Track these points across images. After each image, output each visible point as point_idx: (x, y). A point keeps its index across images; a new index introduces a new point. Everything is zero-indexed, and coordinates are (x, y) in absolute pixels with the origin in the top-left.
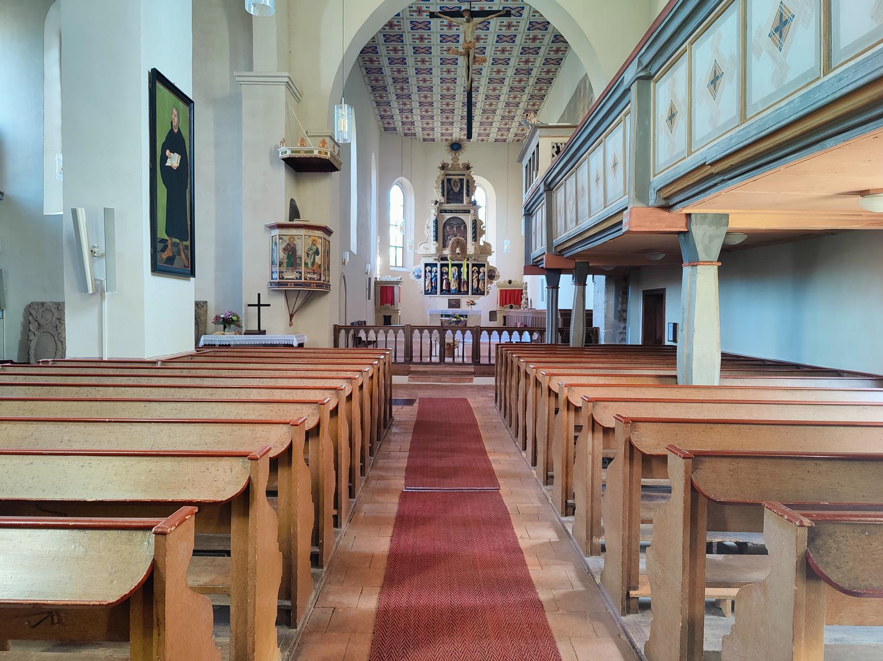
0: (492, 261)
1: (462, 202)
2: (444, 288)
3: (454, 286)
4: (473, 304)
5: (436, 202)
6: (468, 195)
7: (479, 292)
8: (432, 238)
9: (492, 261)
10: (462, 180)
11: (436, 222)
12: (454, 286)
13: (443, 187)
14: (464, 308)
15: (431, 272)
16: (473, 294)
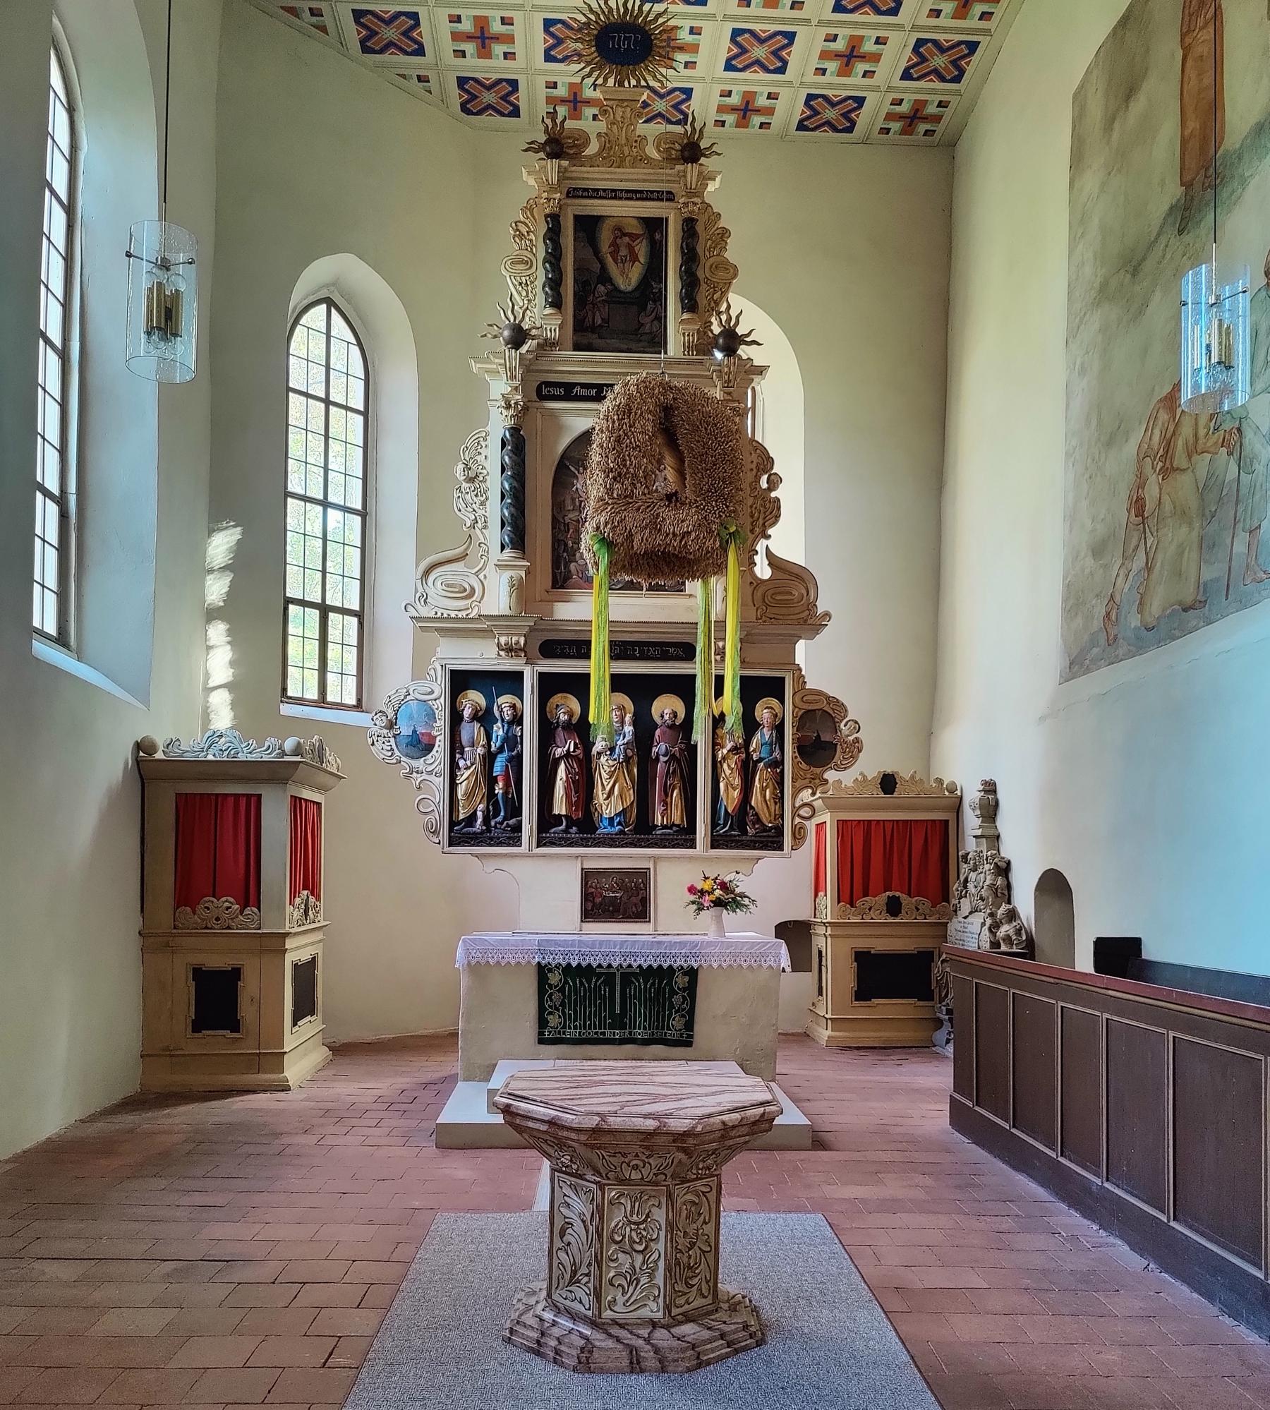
0: (816, 663)
1: (657, 342)
2: (560, 807)
3: (611, 800)
4: (727, 899)
5: (518, 337)
6: (689, 303)
7: (749, 831)
8: (494, 535)
9: (816, 663)
10: (654, 226)
11: (517, 445)
12: (611, 800)
13: (554, 258)
14: (674, 925)
15: (485, 718)
16: (715, 844)
